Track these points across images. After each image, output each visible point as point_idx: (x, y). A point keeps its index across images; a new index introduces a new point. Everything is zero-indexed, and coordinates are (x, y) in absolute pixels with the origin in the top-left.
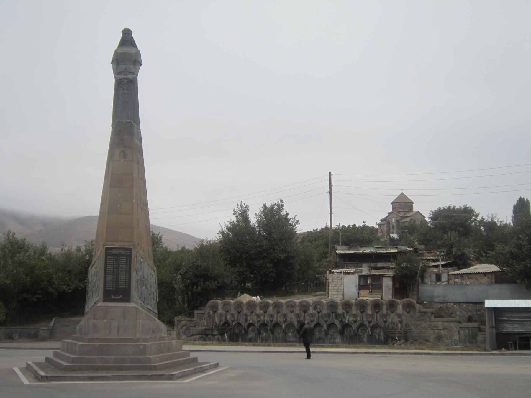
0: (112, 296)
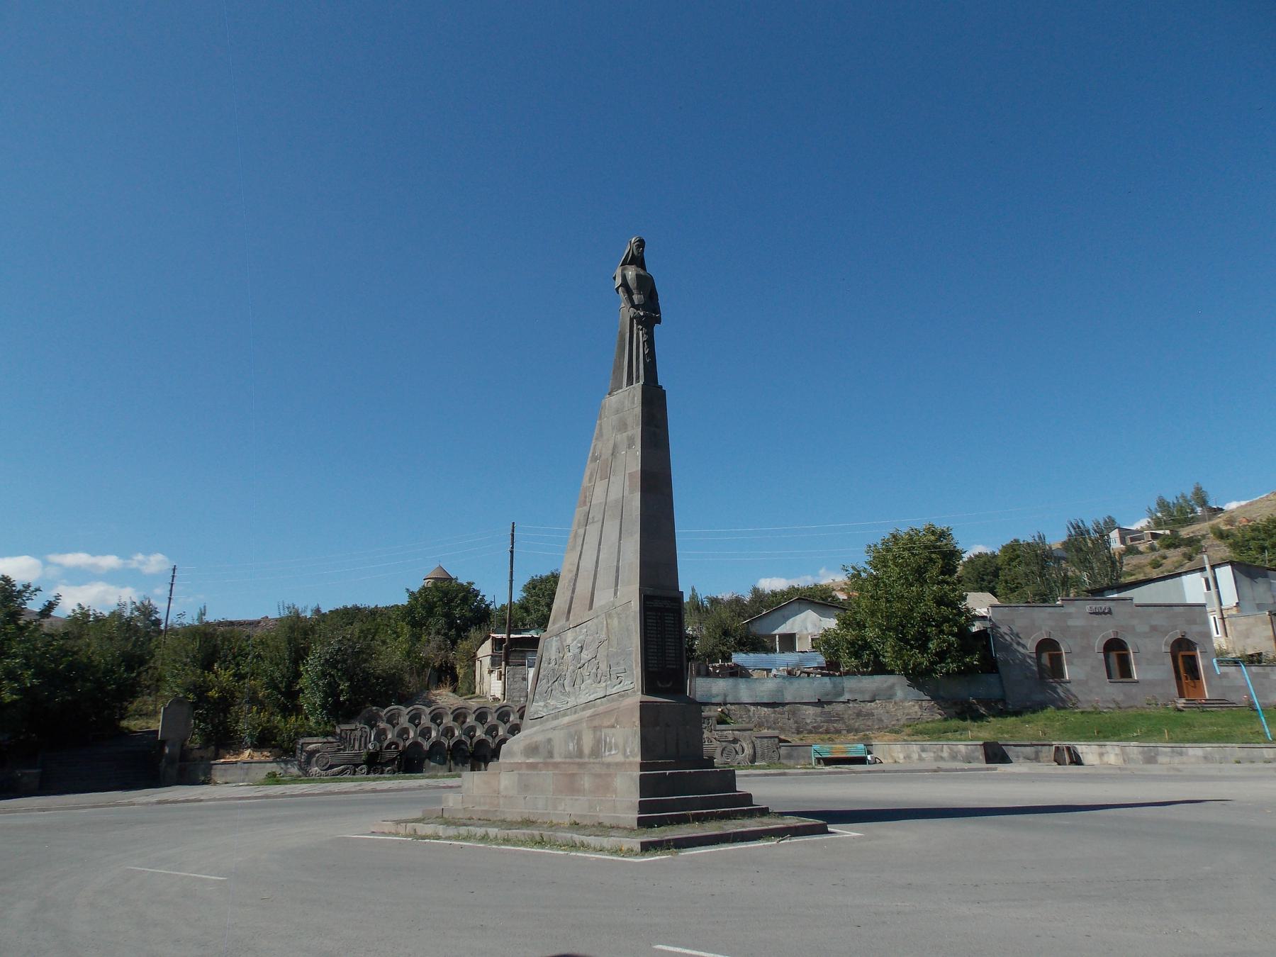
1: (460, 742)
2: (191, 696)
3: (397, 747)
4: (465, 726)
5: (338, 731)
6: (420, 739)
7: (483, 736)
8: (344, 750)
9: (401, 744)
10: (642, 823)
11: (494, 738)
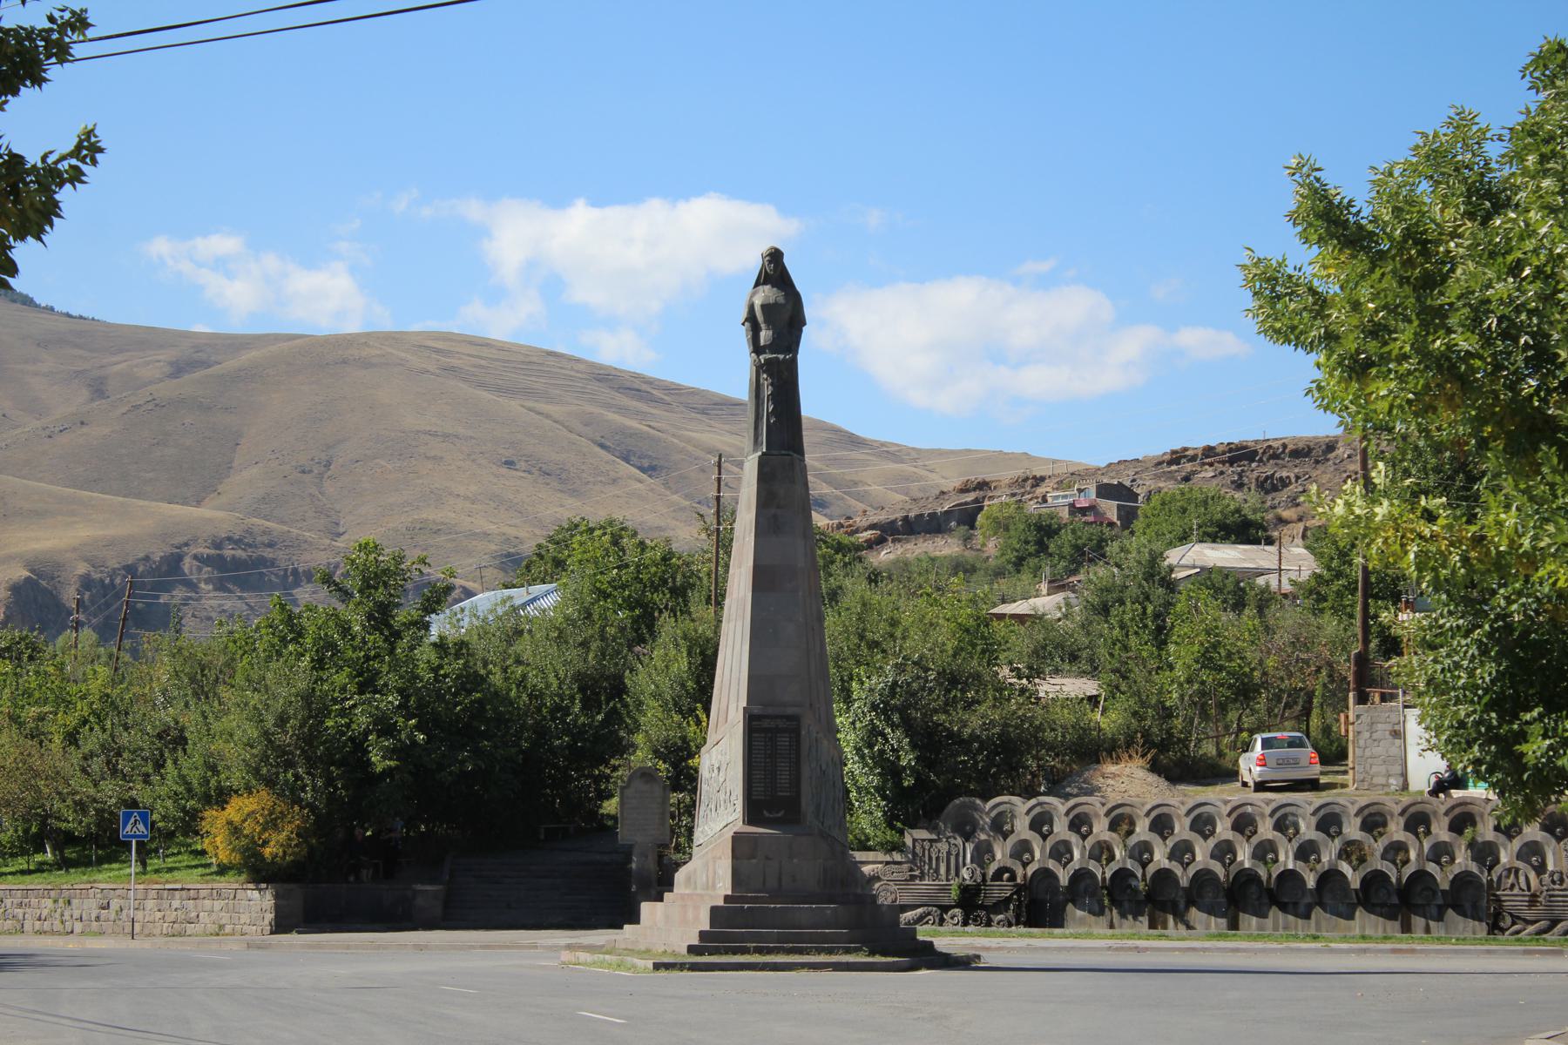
1: (1122, 875)
2: (662, 766)
3: (1013, 878)
4: (1132, 840)
5: (908, 841)
6: (1052, 864)
7: (1166, 864)
8: (922, 878)
9: (1020, 872)
10: (692, 950)
11: (1185, 866)
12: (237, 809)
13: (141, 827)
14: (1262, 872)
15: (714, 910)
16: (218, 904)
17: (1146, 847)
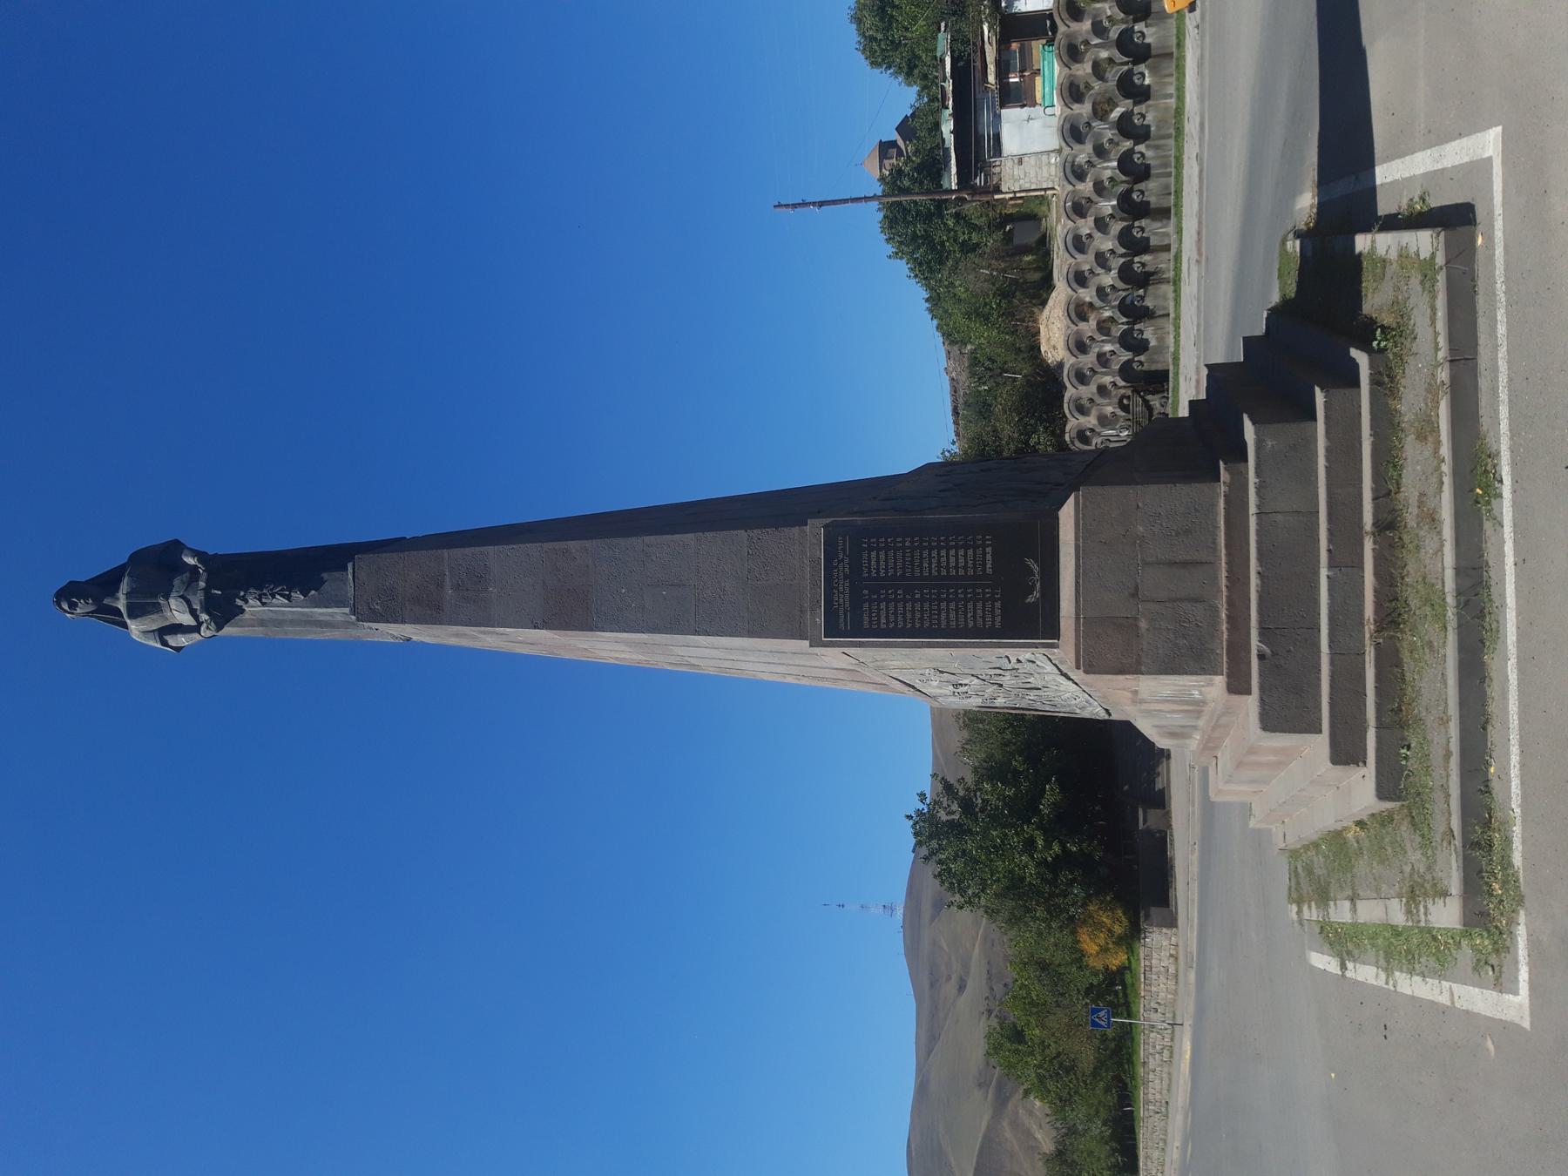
0: (1031, 599)
4: (1098, 303)
7: (1114, 273)
12: (1091, 947)
13: (1102, 1014)
14: (1121, 188)
15: (1272, 721)
16: (1155, 955)
17: (1101, 292)
